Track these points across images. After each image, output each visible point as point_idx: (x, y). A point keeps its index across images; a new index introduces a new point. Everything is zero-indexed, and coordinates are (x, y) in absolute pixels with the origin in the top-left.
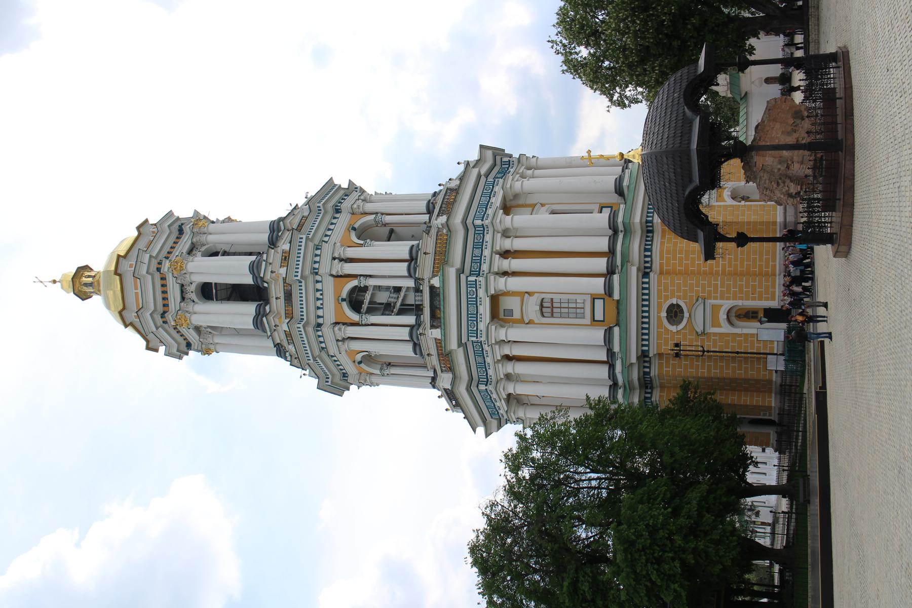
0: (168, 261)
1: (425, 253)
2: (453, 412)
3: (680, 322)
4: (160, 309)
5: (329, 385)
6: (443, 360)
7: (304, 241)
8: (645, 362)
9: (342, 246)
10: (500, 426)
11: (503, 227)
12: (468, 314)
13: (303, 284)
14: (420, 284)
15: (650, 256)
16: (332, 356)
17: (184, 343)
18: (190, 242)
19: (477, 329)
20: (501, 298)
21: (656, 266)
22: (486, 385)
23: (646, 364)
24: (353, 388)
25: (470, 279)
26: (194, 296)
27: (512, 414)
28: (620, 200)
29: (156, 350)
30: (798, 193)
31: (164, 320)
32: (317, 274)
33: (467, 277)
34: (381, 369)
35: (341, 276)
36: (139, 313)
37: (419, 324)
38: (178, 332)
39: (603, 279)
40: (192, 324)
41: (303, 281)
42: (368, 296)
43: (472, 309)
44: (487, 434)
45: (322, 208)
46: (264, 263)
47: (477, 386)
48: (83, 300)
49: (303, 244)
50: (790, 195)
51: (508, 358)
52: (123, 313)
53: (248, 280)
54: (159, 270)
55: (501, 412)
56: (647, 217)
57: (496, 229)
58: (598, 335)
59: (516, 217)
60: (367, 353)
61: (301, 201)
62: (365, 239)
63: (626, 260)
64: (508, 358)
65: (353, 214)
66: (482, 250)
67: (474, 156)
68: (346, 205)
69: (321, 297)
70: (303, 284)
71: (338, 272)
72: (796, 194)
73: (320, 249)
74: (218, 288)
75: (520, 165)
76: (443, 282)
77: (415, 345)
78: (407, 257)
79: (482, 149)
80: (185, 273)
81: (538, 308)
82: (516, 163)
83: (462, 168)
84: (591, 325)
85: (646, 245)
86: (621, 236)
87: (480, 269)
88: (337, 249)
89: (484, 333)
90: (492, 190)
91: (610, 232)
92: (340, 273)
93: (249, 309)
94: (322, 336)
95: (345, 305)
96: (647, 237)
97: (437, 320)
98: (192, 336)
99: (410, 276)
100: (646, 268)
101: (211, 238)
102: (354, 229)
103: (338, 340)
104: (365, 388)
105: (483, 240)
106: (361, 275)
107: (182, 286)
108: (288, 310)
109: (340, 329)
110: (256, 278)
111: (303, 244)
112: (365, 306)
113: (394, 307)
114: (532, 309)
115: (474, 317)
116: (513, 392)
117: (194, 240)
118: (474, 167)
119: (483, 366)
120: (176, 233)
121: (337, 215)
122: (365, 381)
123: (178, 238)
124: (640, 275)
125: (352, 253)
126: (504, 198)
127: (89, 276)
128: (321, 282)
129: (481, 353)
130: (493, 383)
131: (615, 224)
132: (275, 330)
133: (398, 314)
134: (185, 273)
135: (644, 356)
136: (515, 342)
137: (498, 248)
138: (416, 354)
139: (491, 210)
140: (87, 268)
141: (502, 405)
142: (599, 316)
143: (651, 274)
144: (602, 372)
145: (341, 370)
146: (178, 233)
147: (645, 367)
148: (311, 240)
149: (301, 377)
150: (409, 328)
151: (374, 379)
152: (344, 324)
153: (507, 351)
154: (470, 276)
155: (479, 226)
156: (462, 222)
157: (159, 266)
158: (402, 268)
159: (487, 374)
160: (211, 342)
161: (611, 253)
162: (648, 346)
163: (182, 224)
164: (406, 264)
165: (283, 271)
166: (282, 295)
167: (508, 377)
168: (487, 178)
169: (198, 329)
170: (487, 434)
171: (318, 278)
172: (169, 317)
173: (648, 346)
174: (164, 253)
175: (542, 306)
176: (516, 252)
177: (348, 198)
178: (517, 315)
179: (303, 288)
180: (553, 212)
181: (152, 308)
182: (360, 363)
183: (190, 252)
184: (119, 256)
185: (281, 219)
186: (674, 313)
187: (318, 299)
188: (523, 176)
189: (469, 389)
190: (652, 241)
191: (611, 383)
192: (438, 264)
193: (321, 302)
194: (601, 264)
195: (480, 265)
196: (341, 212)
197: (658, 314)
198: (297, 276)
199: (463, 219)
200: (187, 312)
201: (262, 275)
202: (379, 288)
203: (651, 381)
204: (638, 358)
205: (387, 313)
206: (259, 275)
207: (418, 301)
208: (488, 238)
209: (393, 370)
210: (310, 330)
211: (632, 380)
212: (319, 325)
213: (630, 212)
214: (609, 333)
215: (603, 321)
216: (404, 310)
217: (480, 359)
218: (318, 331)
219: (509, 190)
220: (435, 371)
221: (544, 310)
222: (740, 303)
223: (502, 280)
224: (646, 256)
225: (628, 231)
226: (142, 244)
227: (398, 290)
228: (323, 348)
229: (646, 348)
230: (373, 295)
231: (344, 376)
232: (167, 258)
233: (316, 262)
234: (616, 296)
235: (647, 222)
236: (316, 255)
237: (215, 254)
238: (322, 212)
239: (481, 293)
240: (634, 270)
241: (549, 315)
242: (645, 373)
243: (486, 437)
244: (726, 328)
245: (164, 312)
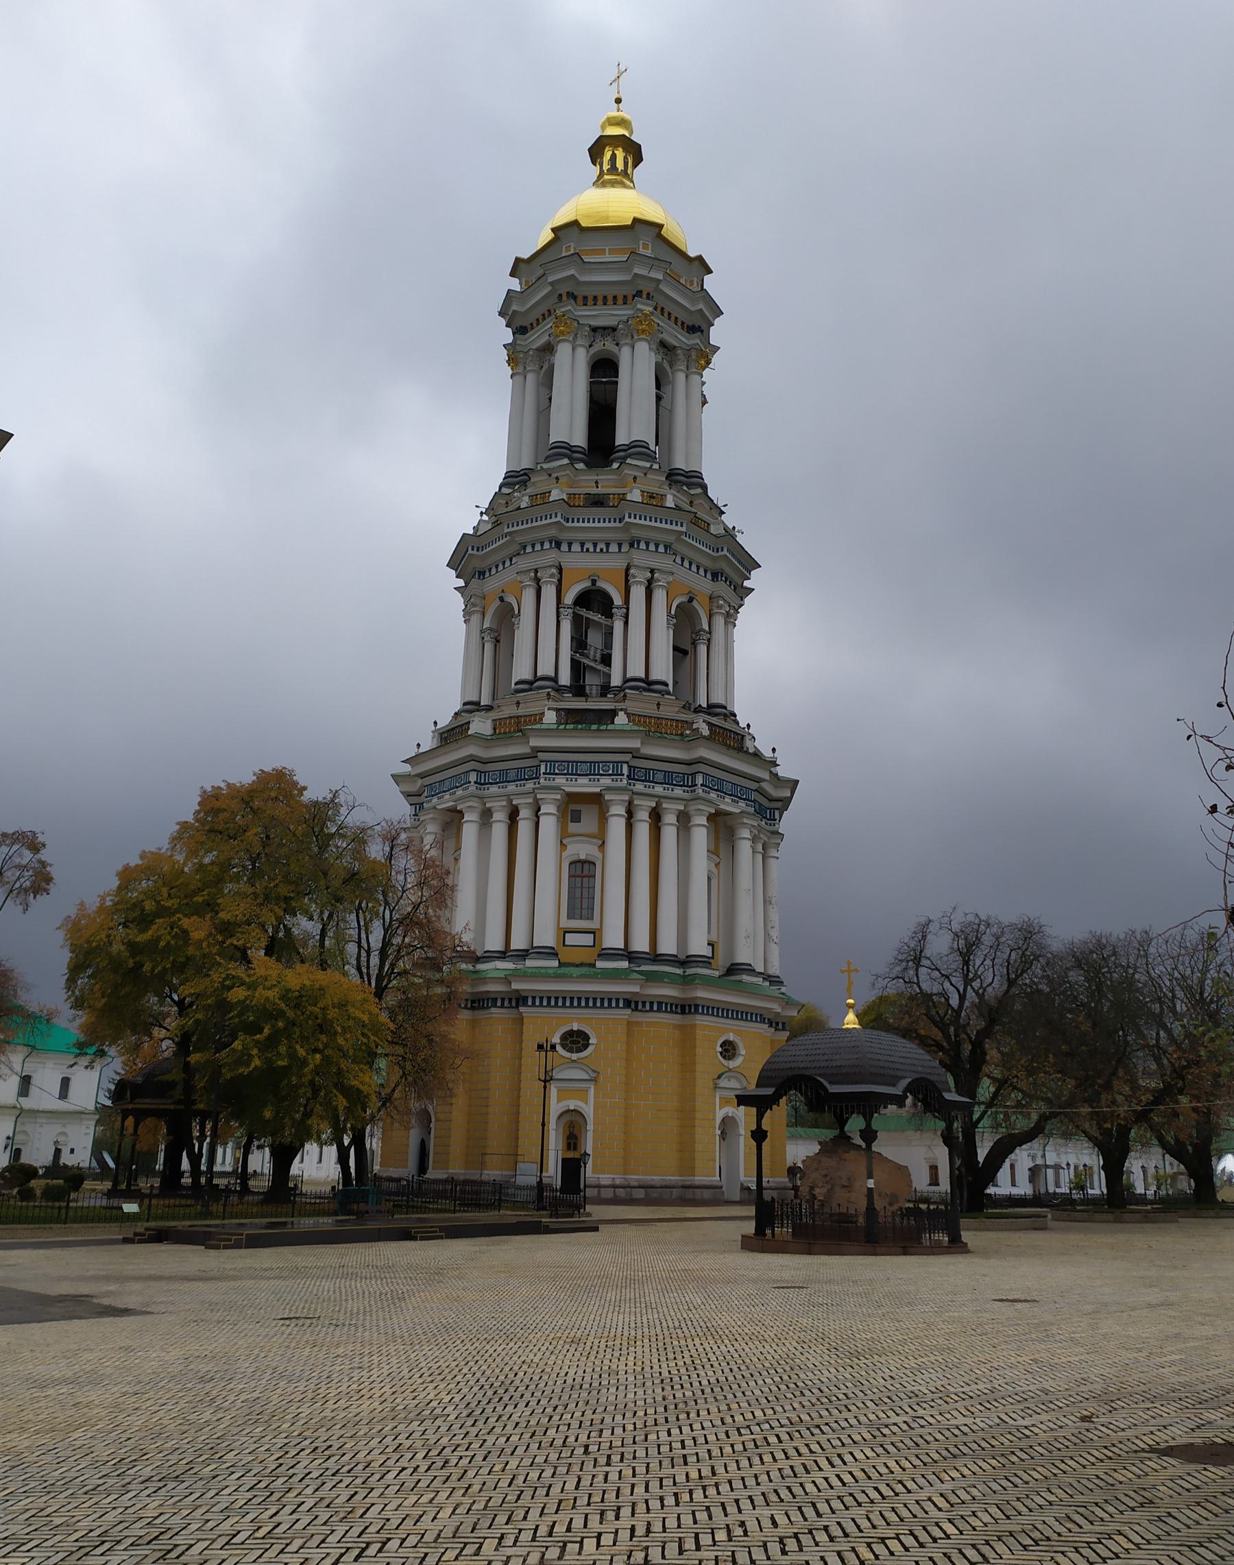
0: (651, 309)
1: (658, 704)
2: (433, 732)
3: (564, 1046)
4: (580, 292)
5: (467, 550)
6: (510, 723)
7: (679, 528)
8: (510, 1000)
9: (667, 583)
10: (408, 795)
11: (692, 813)
12: (577, 762)
13: (617, 524)
14: (615, 695)
15: (651, 1009)
16: (511, 560)
17: (527, 324)
18: (677, 345)
19: (557, 774)
20: (597, 806)
21: (639, 1017)
22: (475, 782)
23: (506, 1003)
24: (461, 583)
25: (625, 767)
26: (598, 346)
27: (431, 816)
28: (722, 971)
29: (512, 274)
30: (814, 1197)
31: (564, 298)
33: (627, 763)
34: (490, 629)
35: (627, 581)
36: (576, 257)
37: (559, 689)
38: (543, 315)
39: (622, 947)
40: (559, 342)
42: (597, 617)
43: (584, 768)
44: (397, 778)
45: (720, 553)
46: (648, 465)
47: (474, 770)
48: (589, 150)
49: (674, 527)
50: (812, 1188)
51: (513, 815)
53: (621, 438)
54: (639, 294)
55: (435, 800)
56: (703, 1007)
57: (690, 803)
58: (546, 937)
59: (704, 831)
61: (729, 520)
62: (676, 616)
63: (651, 977)
64: (513, 815)
66: (662, 783)
67: (782, 771)
68: (722, 588)
69: (598, 550)
71: (634, 577)
72: (814, 1195)
74: (608, 387)
75: (769, 834)
76: (622, 733)
77: (531, 683)
78: (654, 676)
79: (791, 785)
80: (632, 337)
81: (583, 857)
82: (772, 828)
83: (768, 754)
84: (559, 928)
85: (666, 1004)
86: (679, 971)
87: (637, 780)
89: (551, 783)
90: (740, 798)
91: (682, 957)
93: (579, 438)
94: (542, 549)
95: (587, 584)
96: (677, 1005)
97: (571, 717)
98: (537, 338)
99: (626, 680)
100: (637, 1003)
101: (681, 377)
102: (691, 600)
103: (536, 571)
104: (459, 601)
105: (675, 785)
106: (628, 609)
107: (614, 329)
108: (579, 498)
109: (552, 576)
110: (625, 450)
111: (674, 527)
112: (583, 612)
113: (582, 654)
114: (583, 850)
115: (573, 771)
117: (679, 352)
118: (771, 772)
119: (503, 778)
121: (709, 576)
122: (474, 605)
124: (626, 996)
125: (660, 597)
126: (729, 814)
127: (626, 164)
128: (620, 551)
129: (521, 776)
130: (479, 792)
131: (694, 964)
132: (550, 475)
133: (572, 660)
135: (519, 1000)
136: (537, 824)
137: (664, 806)
138: (516, 684)
139: (715, 796)
140: (638, 159)
141: (447, 802)
142: (571, 939)
143: (628, 1011)
144: (494, 943)
145: (490, 570)
146: (690, 324)
147: (503, 1000)
148: (678, 539)
149: (477, 507)
150: (553, 675)
151: (475, 618)
152: (560, 581)
153: (524, 813)
154: (630, 767)
155: (694, 780)
156: (701, 757)
157: (644, 296)
158: (637, 670)
159: (491, 784)
160: (528, 369)
161: (655, 957)
162: (534, 1004)
163: (702, 332)
164: (643, 675)
165: (635, 495)
166: (601, 490)
167: (486, 815)
168: (756, 790)
169: (549, 349)
170: (397, 778)
171: (625, 548)
172: (567, 307)
173: (534, 1004)
174: (663, 303)
175: (583, 862)
176: (659, 829)
177: (730, 590)
178: (573, 827)
180: (709, 879)
182: (501, 599)
183: (663, 345)
184: (661, 226)
185: (704, 487)
186: (576, 1040)
187: (595, 545)
188: (754, 839)
189: (472, 758)
190: (672, 1012)
191: (479, 954)
192: (645, 722)
193: (591, 549)
194: (641, 943)
195: (642, 781)
196: (713, 580)
197: (576, 1020)
198: (630, 517)
199: (705, 759)
200: (576, 335)
201: (629, 461)
202: (609, 633)
203: (483, 1008)
204: (517, 991)
205: (574, 644)
206: (629, 456)
207: (591, 690)
208: (678, 792)
209: (489, 647)
210: (553, 532)
211: (486, 983)
212: (558, 545)
213: (708, 982)
214: (551, 953)
215: (564, 945)
216: (577, 668)
217: (512, 775)
218: (551, 543)
220: (489, 708)
221: (579, 865)
222: (590, 1127)
223: (621, 810)
224: (652, 1003)
225: (687, 981)
226: (678, 265)
227: (607, 660)
228: (524, 548)
229: (530, 1003)
230: (598, 624)
232: (655, 309)
233: (647, 544)
234: (599, 964)
235: (697, 1006)
236: (657, 546)
237: (658, 386)
238: (715, 554)
239: (606, 781)
240: (636, 989)
241: (573, 872)
242: (495, 1000)
243: (392, 776)
244: (555, 1108)
245: (575, 298)
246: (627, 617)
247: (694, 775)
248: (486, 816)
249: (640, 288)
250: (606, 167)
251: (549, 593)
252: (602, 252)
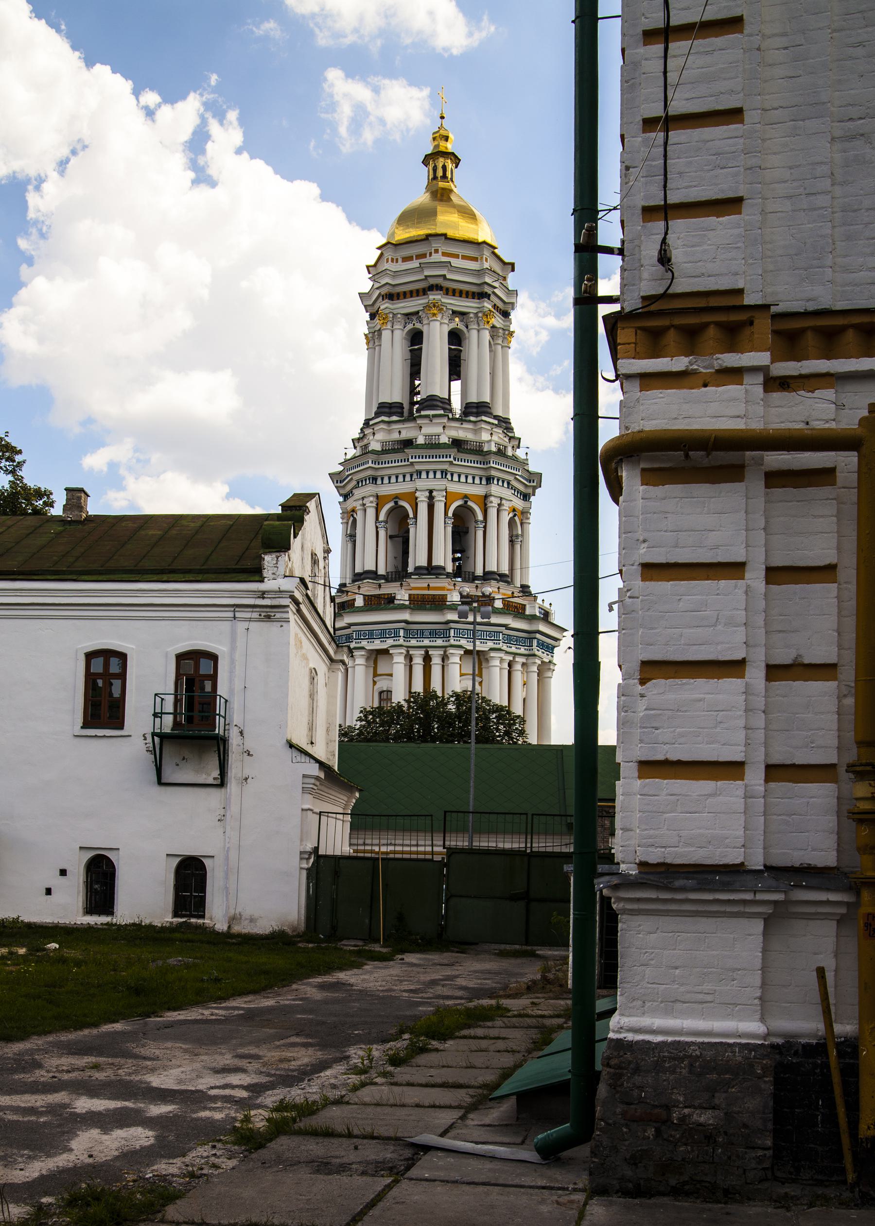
4: (446, 284)
13: (482, 466)
26: (452, 326)
27: (363, 653)
29: (379, 248)
32: (489, 480)
35: (485, 505)
41: (485, 466)
45: (532, 484)
48: (426, 156)
49: (515, 472)
51: (427, 659)
52: (443, 238)
55: (364, 643)
60: (411, 515)
64: (427, 659)
70: (482, 466)
71: (491, 502)
73: (508, 488)
88: (508, 502)
92: (489, 505)
102: (515, 515)
103: (431, 492)
106: (486, 523)
107: (462, 314)
116: (394, 661)
119: (421, 634)
122: (371, 502)
123: (498, 307)
129: (434, 634)
134: (479, 325)
137: (517, 659)
141: (377, 645)
145: (382, 479)
153: (436, 661)
158: (492, 567)
167: (409, 658)
179: (479, 466)
181: (448, 277)
182: (396, 503)
184: (495, 248)
196: (523, 500)
201: (484, 418)
208: (522, 650)
209: (382, 533)
219: (547, 667)
228: (419, 473)
231: (373, 479)
233: (498, 480)
236: (503, 482)
239: (490, 644)
246: (485, 527)
247: (531, 639)
248: (409, 658)
249: (486, 290)
250: (440, 173)
252: (457, 256)
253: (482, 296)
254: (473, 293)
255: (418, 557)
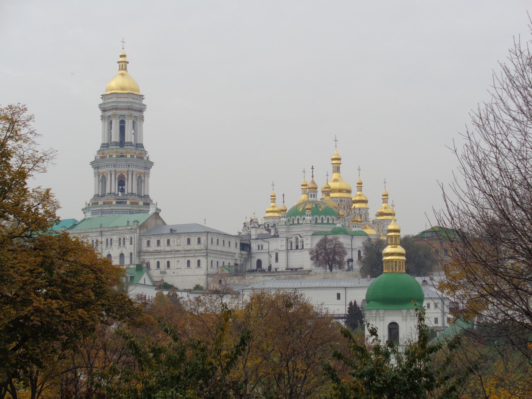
26: (121, 119)
65: (144, 173)
68: (147, 171)
78: (134, 192)
93: (118, 140)
99: (128, 193)
107: (124, 115)
120: (140, 109)
125: (134, 176)
151: (97, 177)
158: (130, 191)
183: (135, 116)
185: (143, 147)
209: (100, 183)
210: (114, 164)
220: (102, 196)
237: (133, 124)
251: (113, 176)
252: (121, 98)
253: (129, 109)
254: (126, 109)
255: (108, 191)
